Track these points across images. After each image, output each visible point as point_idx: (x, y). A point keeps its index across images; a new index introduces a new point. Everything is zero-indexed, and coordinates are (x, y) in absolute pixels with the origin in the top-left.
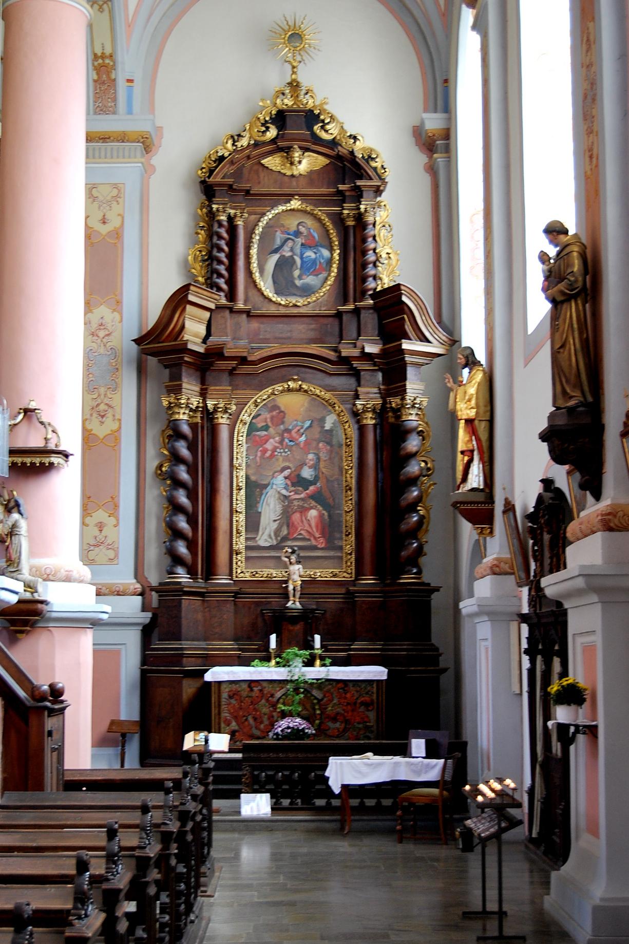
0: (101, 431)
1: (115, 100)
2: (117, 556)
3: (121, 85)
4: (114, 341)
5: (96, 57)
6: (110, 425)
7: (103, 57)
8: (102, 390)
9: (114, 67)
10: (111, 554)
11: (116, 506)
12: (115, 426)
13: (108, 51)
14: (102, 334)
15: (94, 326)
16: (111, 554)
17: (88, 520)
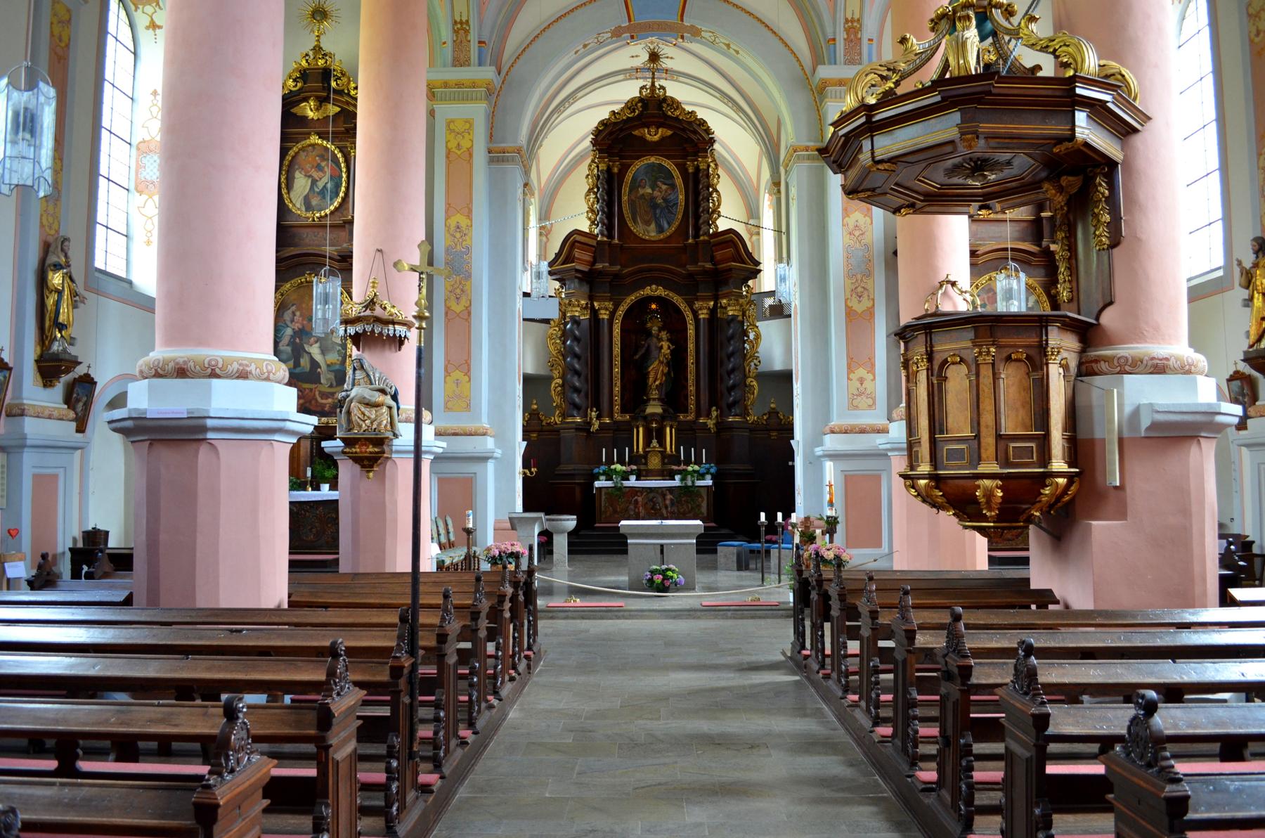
0: (859, 307)
1: (860, 54)
2: (874, 403)
3: (865, 42)
4: (867, 239)
5: (847, 21)
6: (866, 303)
7: (852, 21)
8: (859, 277)
9: (860, 29)
10: (870, 402)
11: (873, 365)
12: (870, 305)
13: (857, 16)
14: (857, 233)
15: (851, 227)
16: (870, 402)
17: (852, 376)
